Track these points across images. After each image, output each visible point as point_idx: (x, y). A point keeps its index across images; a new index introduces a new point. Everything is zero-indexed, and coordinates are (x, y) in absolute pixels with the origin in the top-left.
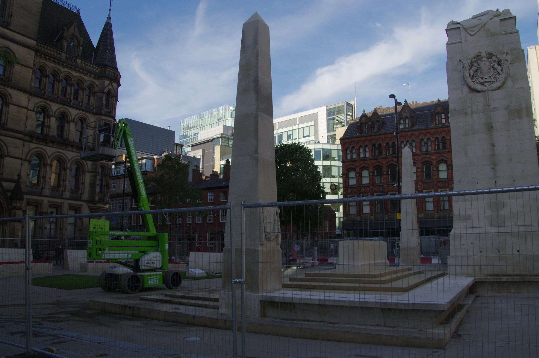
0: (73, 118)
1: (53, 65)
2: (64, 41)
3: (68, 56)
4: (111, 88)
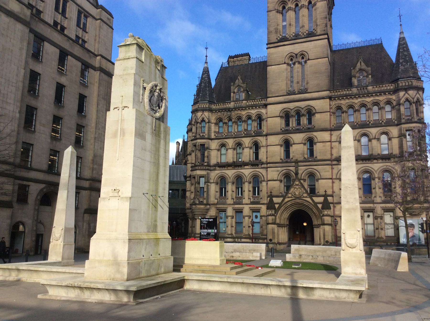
0: (374, 135)
2: (353, 78)
3: (359, 88)
4: (408, 96)
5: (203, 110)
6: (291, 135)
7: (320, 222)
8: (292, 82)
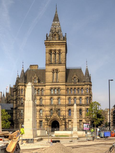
5: (22, 86)
6: (53, 96)
8: (53, 78)
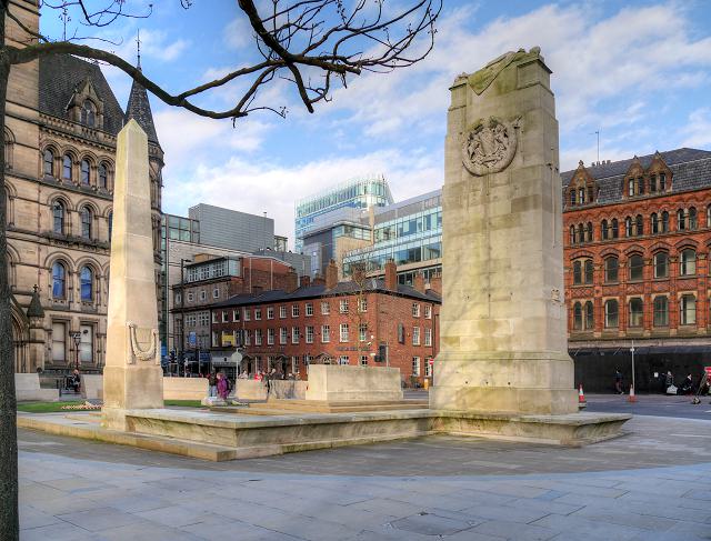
1: (66, 142)
2: (77, 108)
7: (24, 337)
